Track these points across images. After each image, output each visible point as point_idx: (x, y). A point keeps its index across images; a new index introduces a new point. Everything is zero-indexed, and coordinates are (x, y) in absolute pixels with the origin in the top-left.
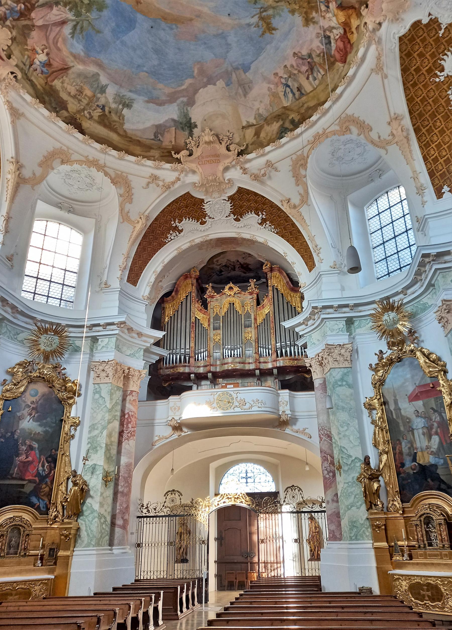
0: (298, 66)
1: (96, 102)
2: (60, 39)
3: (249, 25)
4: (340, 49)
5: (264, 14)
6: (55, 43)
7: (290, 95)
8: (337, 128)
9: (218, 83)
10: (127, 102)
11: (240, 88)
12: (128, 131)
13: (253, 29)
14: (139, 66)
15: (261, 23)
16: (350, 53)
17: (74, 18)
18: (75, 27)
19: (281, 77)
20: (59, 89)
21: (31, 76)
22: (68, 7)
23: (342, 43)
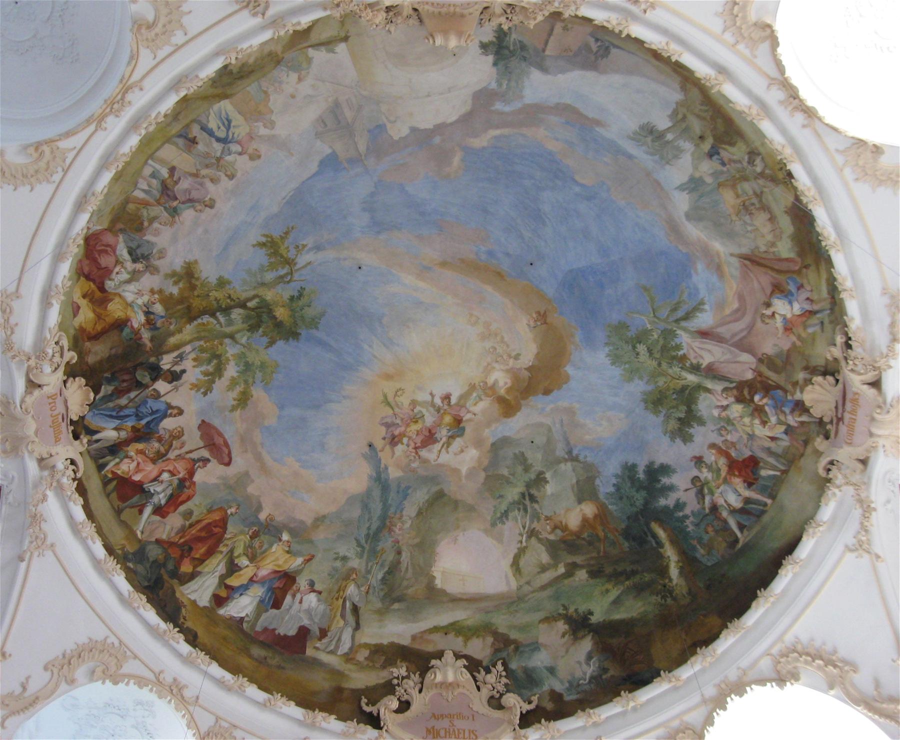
0: (202, 184)
1: (722, 173)
2: (728, 311)
3: (318, 248)
4: (106, 252)
5: (282, 272)
6: (739, 313)
7: (213, 124)
8: (64, 144)
9: (405, 131)
10: (649, 139)
11: (350, 120)
12: (677, 86)
13: (309, 241)
14: (589, 199)
15: (291, 254)
16: (80, 261)
17: (678, 332)
18: (687, 317)
19: (240, 154)
20: (789, 241)
21: (825, 300)
22: (681, 353)
23: (103, 266)
